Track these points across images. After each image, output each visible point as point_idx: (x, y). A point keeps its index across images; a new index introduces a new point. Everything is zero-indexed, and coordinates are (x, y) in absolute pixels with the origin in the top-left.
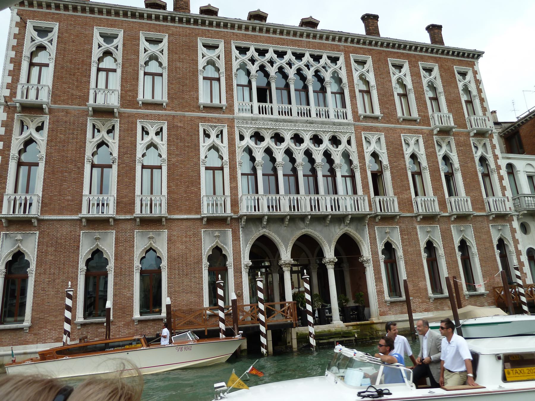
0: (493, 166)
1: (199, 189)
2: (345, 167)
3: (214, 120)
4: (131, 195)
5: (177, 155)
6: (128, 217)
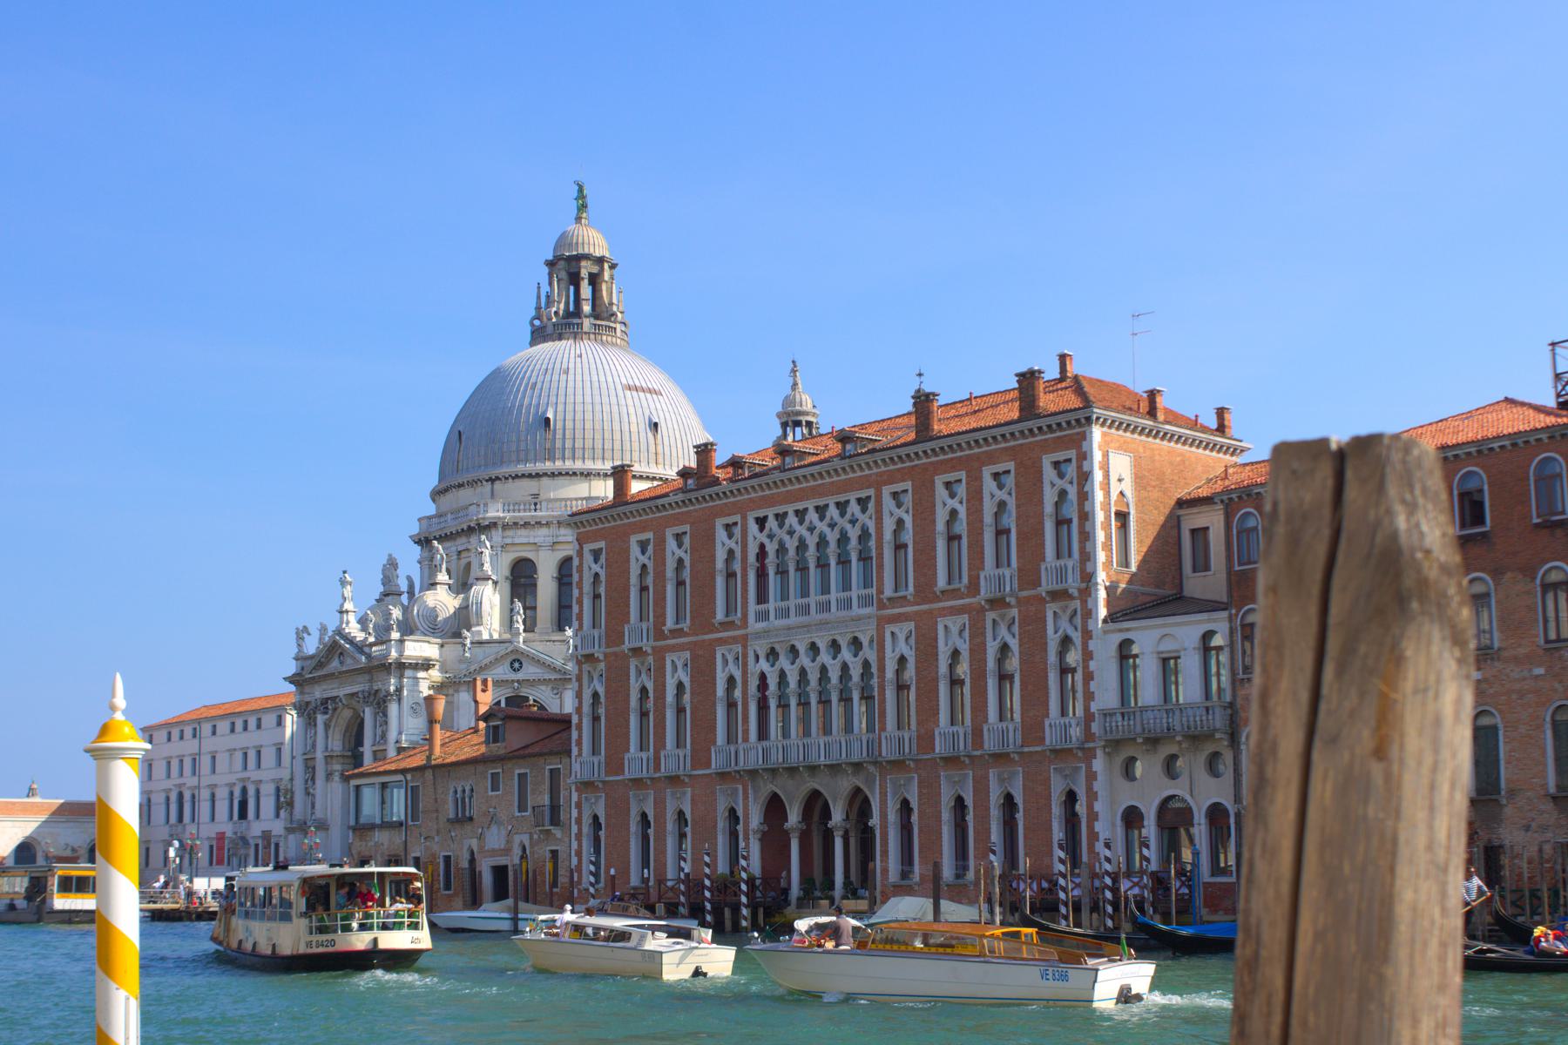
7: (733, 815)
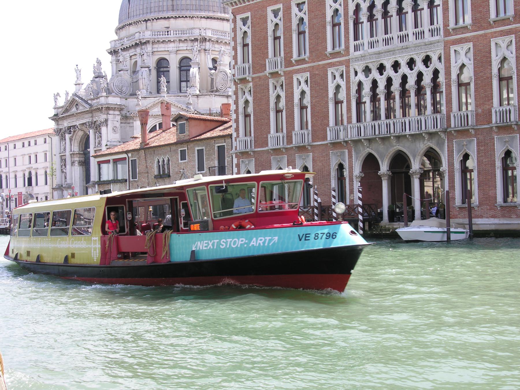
3: (337, 64)
5: (316, 97)
7: (341, 167)
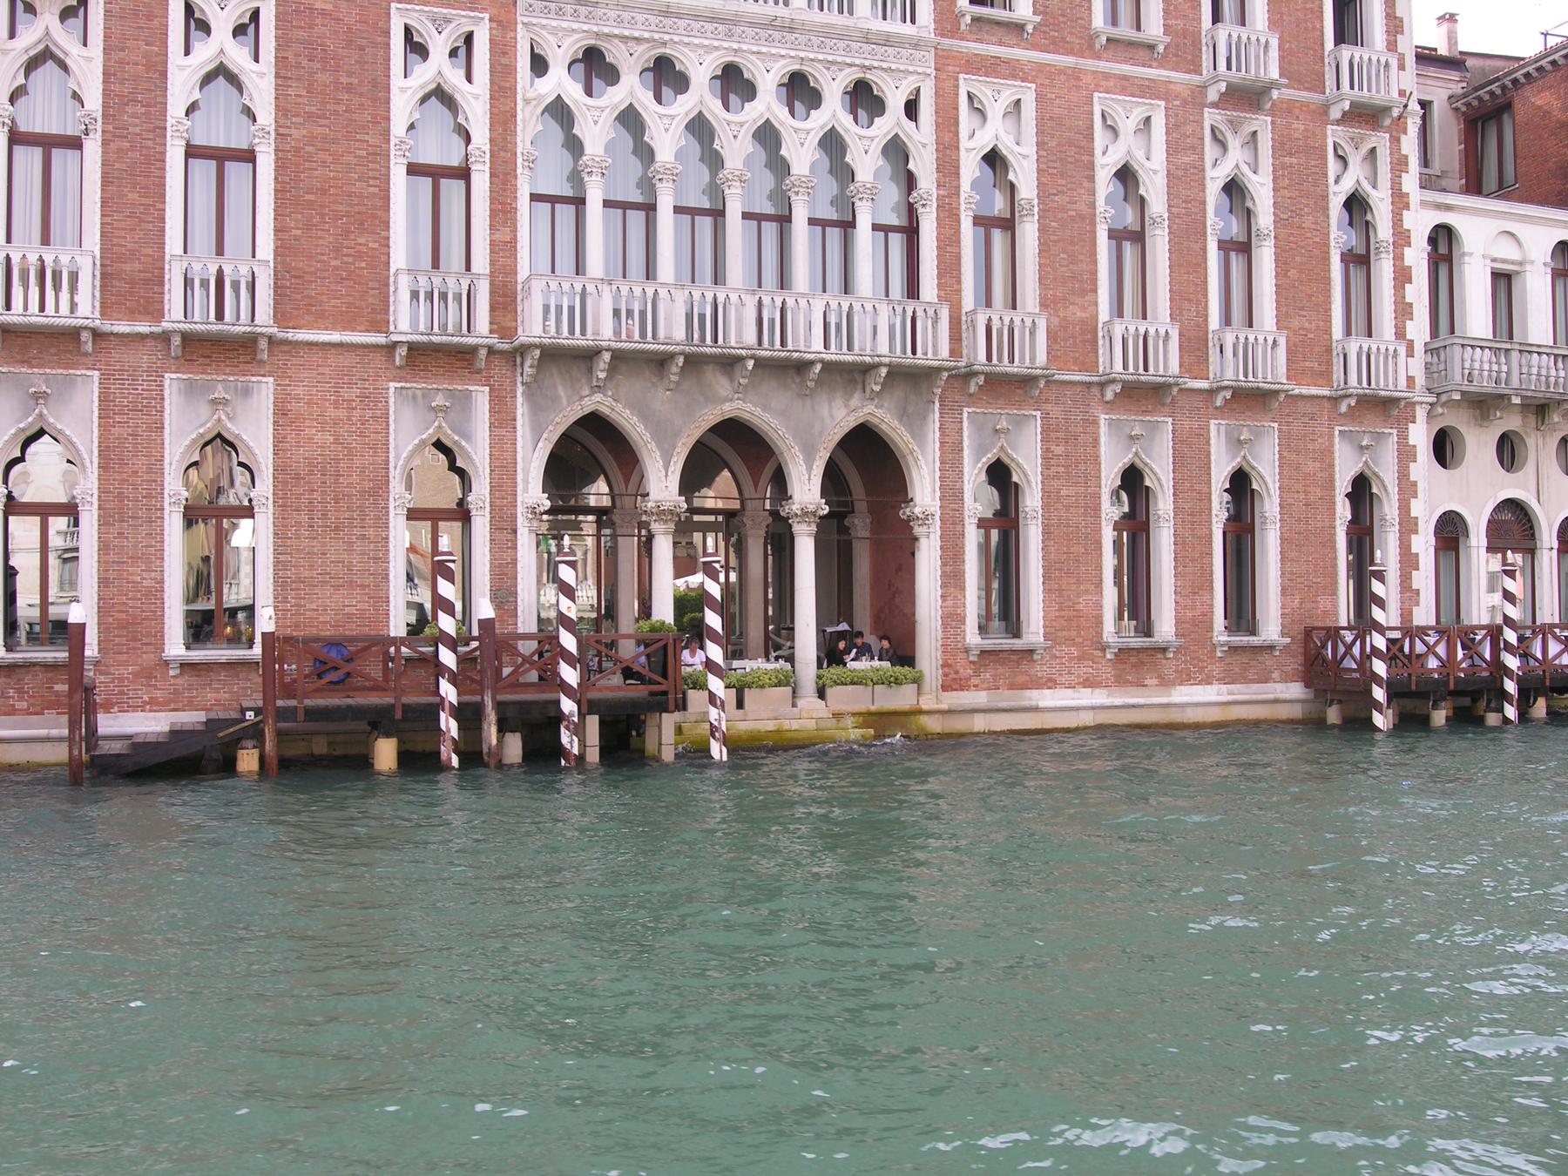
0: (1384, 231)
1: (385, 243)
2: (892, 193)
4: (149, 251)
5: (310, 115)
6: (143, 328)
